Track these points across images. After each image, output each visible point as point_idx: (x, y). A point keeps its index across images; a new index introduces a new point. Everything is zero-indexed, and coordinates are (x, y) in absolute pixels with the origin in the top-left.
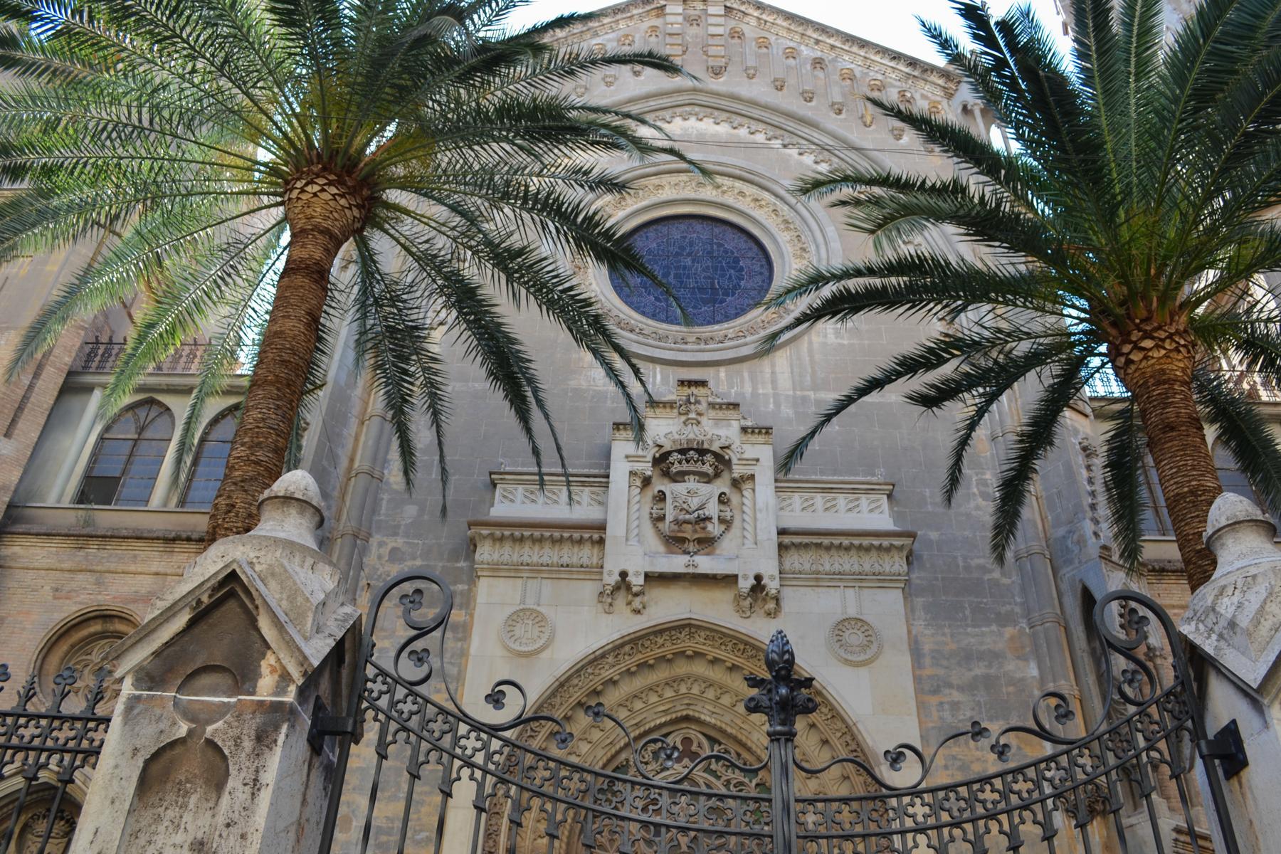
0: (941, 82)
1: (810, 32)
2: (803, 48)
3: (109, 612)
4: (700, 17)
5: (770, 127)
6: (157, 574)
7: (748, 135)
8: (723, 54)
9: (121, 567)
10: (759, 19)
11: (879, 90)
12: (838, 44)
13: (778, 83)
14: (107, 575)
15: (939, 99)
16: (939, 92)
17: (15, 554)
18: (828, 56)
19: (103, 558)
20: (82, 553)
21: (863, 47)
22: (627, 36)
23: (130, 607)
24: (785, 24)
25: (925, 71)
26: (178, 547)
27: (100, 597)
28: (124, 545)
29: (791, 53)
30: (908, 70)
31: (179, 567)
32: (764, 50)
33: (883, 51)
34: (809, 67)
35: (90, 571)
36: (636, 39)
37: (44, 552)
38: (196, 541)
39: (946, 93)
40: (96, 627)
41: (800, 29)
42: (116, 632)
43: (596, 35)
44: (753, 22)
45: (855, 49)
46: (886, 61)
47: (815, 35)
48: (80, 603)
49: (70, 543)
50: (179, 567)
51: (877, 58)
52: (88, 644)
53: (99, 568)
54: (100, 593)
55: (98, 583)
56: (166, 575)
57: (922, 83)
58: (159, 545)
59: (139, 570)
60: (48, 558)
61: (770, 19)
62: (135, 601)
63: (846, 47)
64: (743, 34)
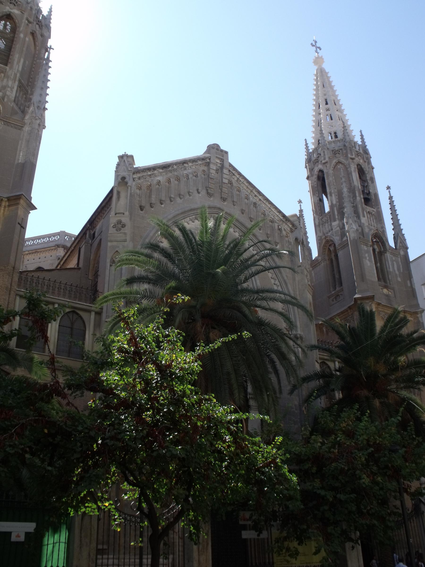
0: (290, 226)
1: (254, 191)
2: (250, 196)
4: (218, 170)
5: (240, 231)
7: (233, 232)
8: (227, 192)
10: (238, 179)
11: (272, 222)
12: (262, 199)
13: (243, 211)
15: (288, 232)
16: (289, 229)
18: (259, 203)
21: (270, 204)
22: (195, 172)
24: (247, 184)
25: (286, 220)
29: (247, 198)
30: (282, 218)
32: (238, 193)
33: (276, 208)
34: (252, 206)
36: (199, 175)
39: (291, 230)
41: (251, 188)
43: (185, 169)
44: (236, 179)
45: (267, 203)
46: (276, 212)
47: (256, 193)
51: (273, 210)
57: (284, 224)
61: (242, 180)
63: (265, 202)
64: (232, 183)
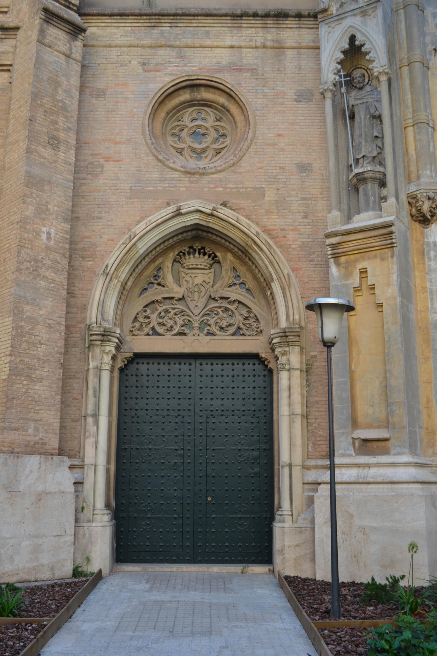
3: (198, 82)
6: (232, 47)
9: (197, 42)
14: (186, 49)
17: (94, 34)
19: (177, 34)
20: (156, 31)
23: (218, 75)
26: (245, 22)
27: (186, 69)
28: (195, 22)
31: (251, 40)
35: (169, 46)
37: (121, 31)
38: (262, 17)
40: (185, 96)
42: (203, 100)
48: (171, 75)
49: (143, 21)
50: (251, 40)
52: (178, 111)
53: (177, 43)
54: (185, 65)
55: (180, 56)
56: (241, 47)
58: (228, 21)
59: (215, 44)
60: (126, 36)
62: (220, 71)
